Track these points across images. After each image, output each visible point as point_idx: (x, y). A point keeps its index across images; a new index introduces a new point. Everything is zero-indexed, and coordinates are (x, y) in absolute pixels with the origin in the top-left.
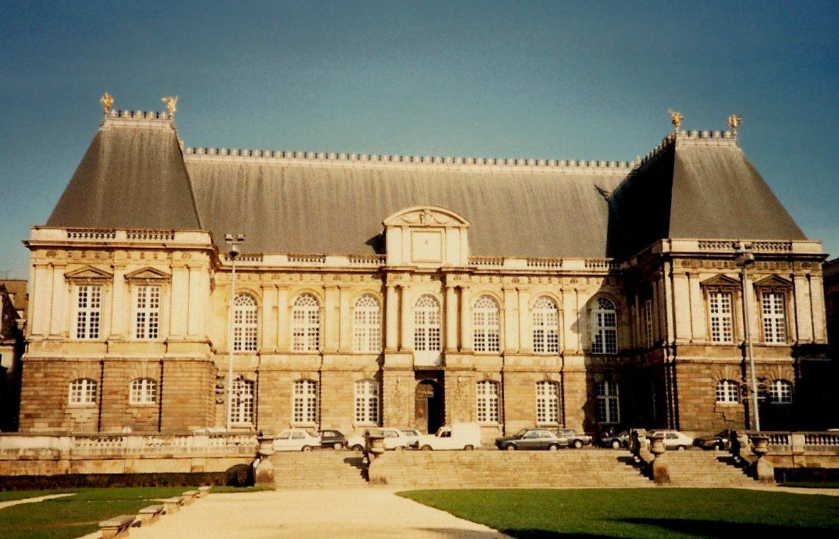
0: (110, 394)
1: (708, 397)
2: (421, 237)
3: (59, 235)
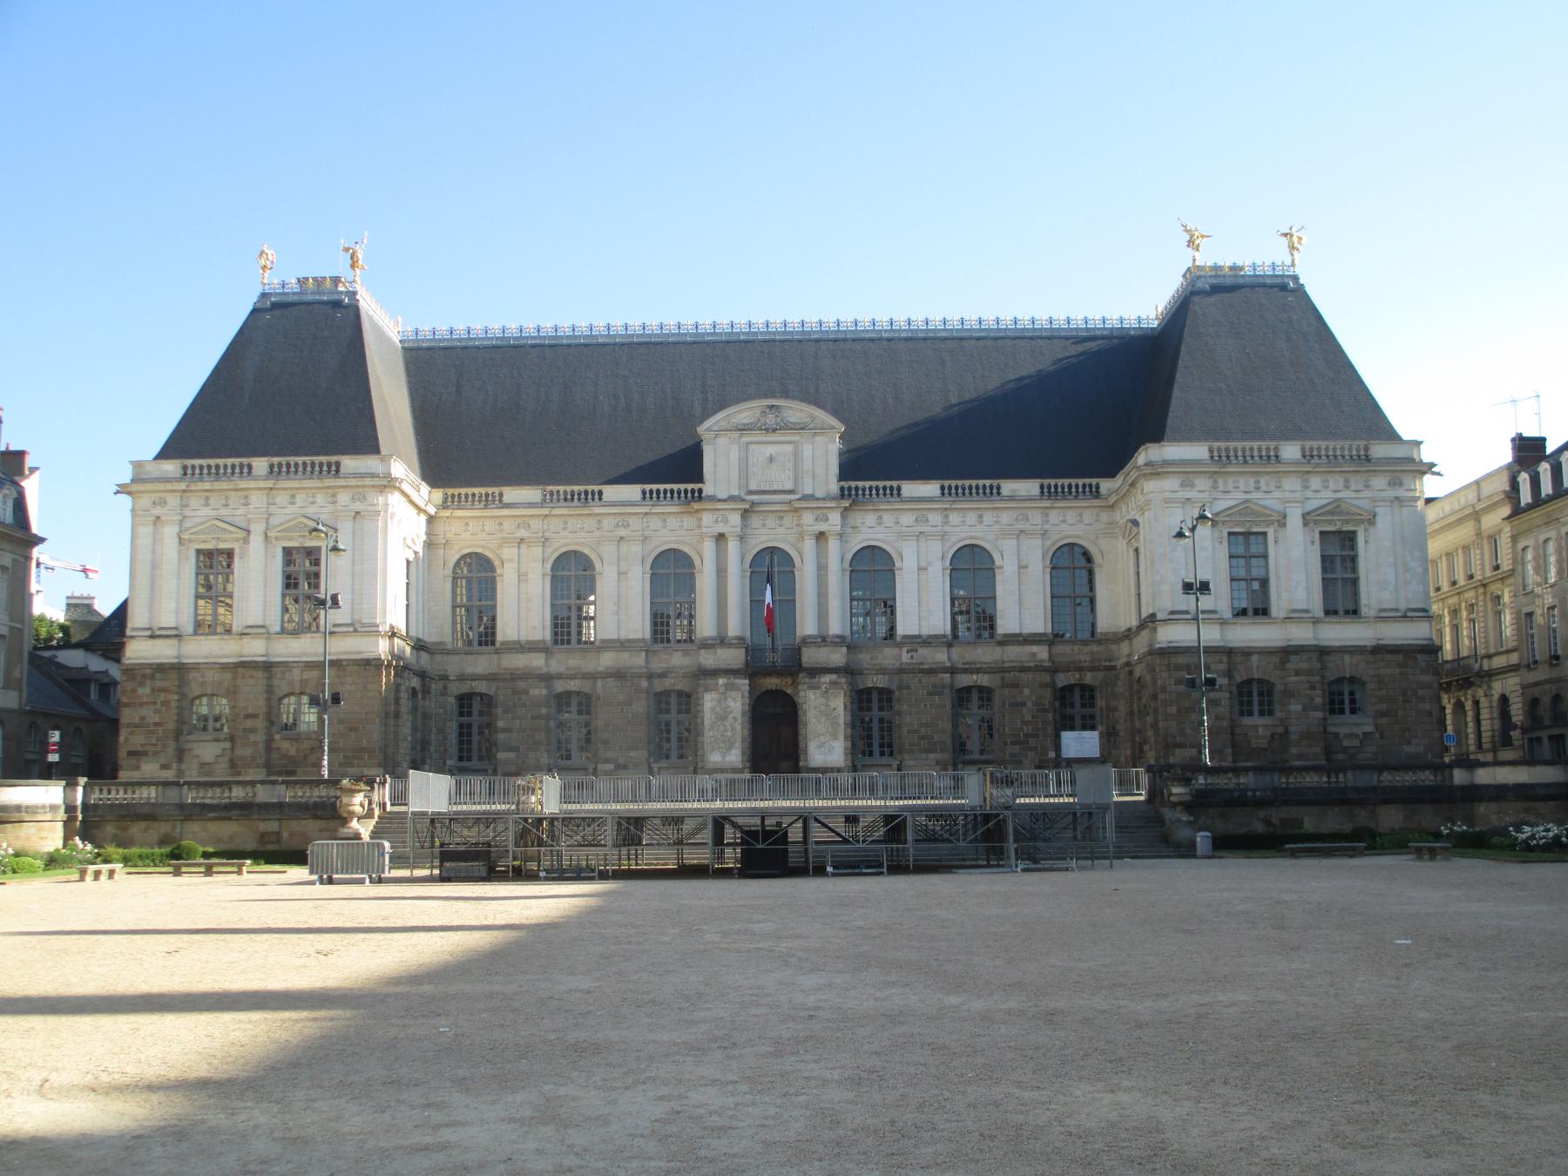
0: (248, 716)
1: (1220, 709)
2: (764, 449)
3: (171, 467)
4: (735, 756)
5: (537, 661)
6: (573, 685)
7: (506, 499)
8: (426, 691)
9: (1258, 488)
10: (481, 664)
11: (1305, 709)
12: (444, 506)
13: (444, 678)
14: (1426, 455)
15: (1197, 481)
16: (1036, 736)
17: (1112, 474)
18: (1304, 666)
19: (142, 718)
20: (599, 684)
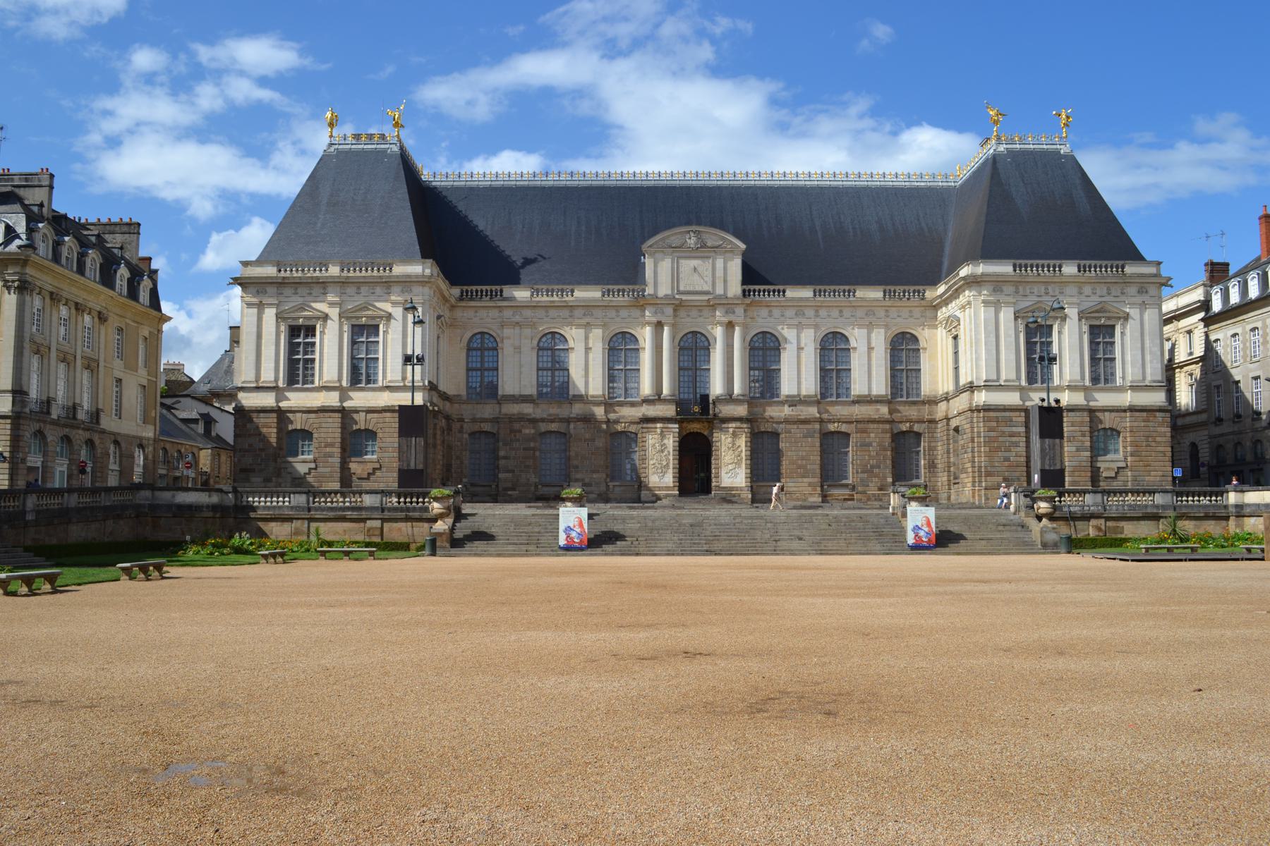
2: (687, 265)
4: (669, 479)
5: (527, 409)
6: (554, 427)
7: (505, 294)
8: (449, 429)
9: (1047, 293)
10: (488, 410)
11: (1078, 450)
12: (461, 299)
13: (461, 420)
14: (1165, 272)
15: (1005, 288)
16: (879, 467)
17: (934, 282)
18: (1079, 419)
19: (250, 445)
20: (572, 426)
